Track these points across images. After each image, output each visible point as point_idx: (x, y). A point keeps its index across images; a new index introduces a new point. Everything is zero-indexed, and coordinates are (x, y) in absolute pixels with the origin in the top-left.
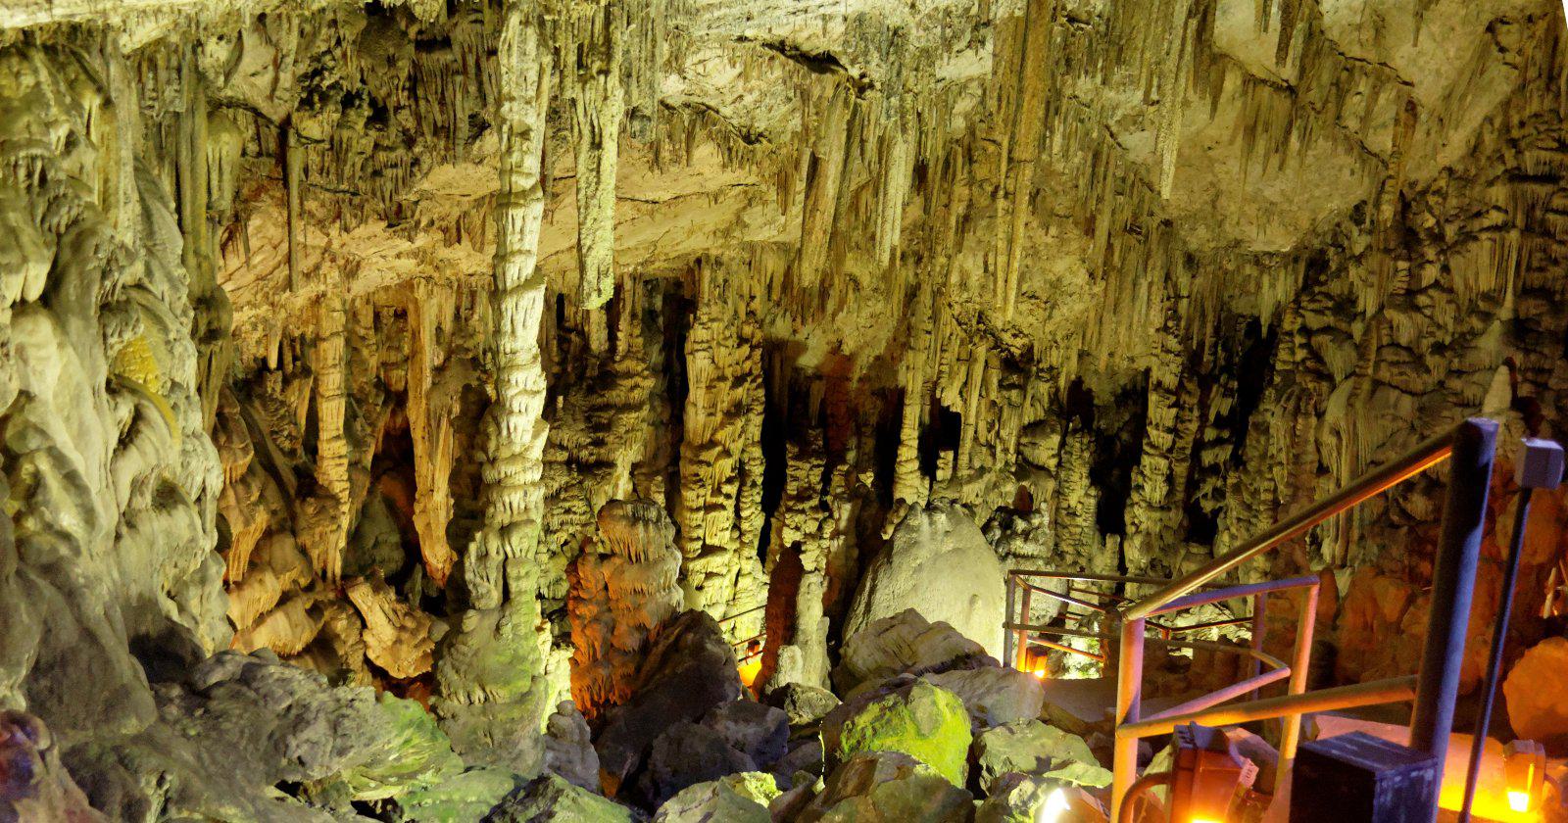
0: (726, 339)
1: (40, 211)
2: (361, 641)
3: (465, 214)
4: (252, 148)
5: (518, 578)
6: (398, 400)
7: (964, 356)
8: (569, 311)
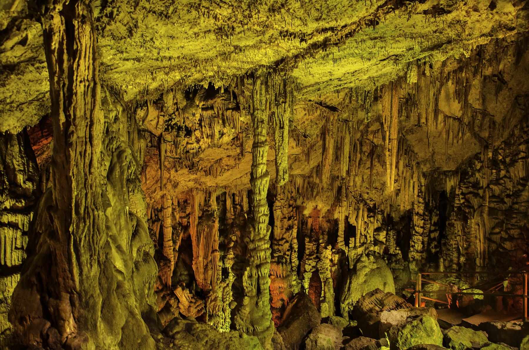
1: (106, 142)
2: (178, 307)
3: (212, 166)
4: (150, 144)
5: (264, 284)
6: (186, 228)
7: (356, 208)
8: (237, 198)
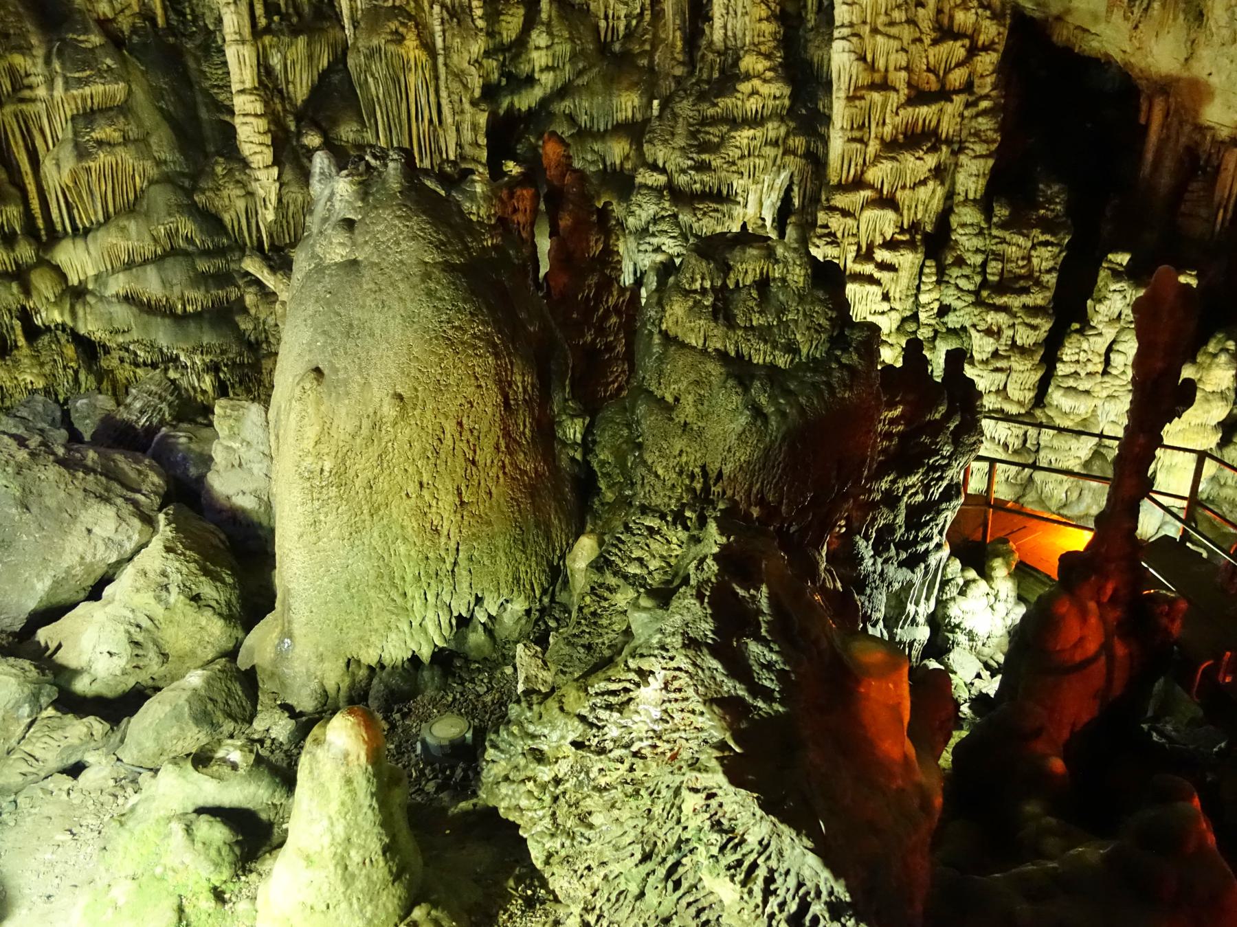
0: (892, 24)
